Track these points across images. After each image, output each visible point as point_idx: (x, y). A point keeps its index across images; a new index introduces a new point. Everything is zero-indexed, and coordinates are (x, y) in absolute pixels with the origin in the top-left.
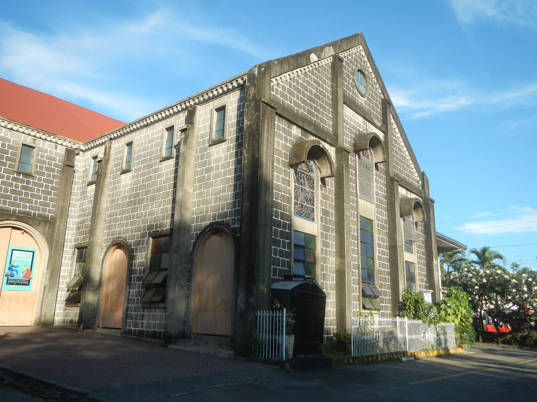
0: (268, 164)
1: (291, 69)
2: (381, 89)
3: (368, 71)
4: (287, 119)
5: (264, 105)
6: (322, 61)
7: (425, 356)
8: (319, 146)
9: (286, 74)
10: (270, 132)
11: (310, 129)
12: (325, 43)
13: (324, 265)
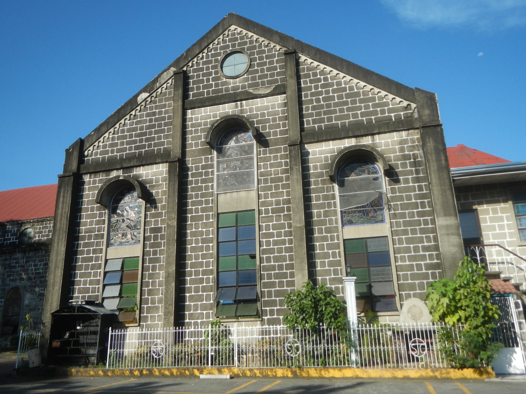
0: (63, 220)
1: (110, 126)
2: (279, 44)
3: (251, 42)
4: (103, 171)
5: (61, 178)
6: (159, 90)
7: (290, 375)
8: (119, 180)
9: (106, 135)
10: (66, 196)
11: (132, 164)
12: (162, 71)
13: (151, 281)
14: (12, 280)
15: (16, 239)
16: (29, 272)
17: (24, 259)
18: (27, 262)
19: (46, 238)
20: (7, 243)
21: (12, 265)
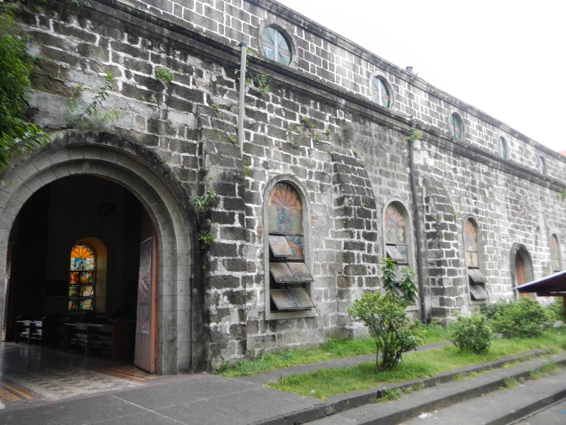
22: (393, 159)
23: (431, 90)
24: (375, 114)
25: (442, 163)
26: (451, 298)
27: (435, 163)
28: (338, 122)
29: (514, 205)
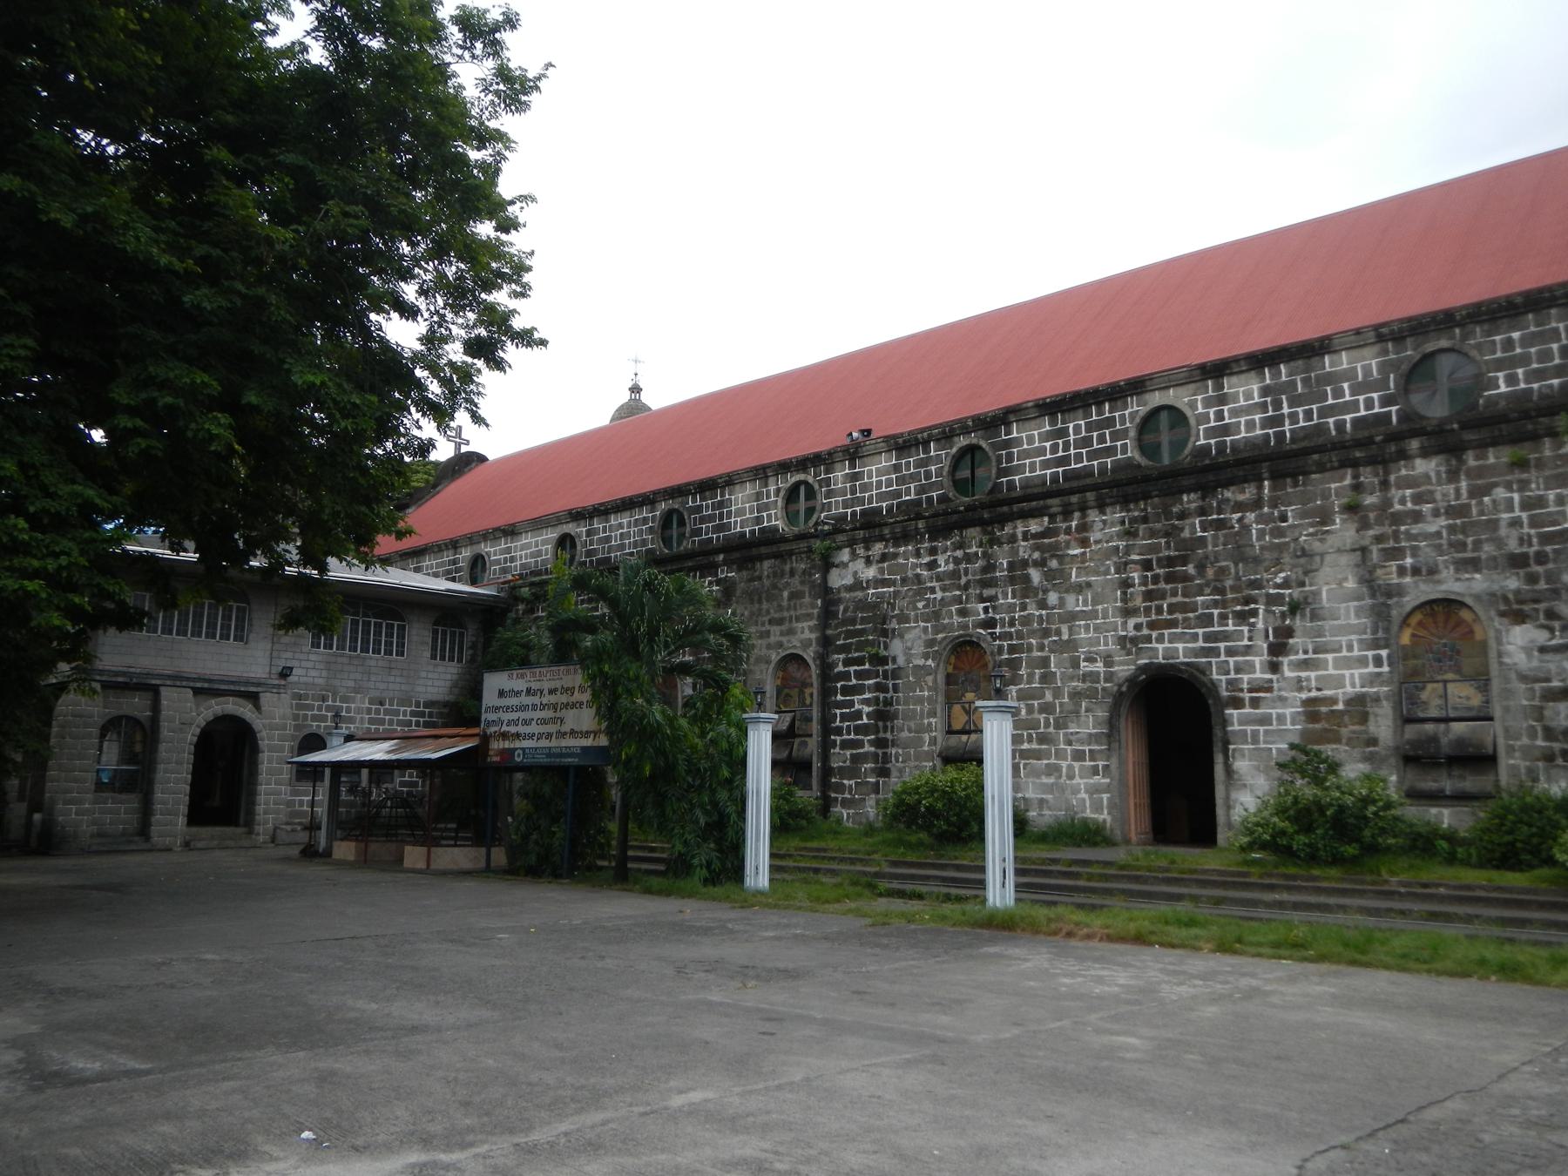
14: (1416, 571)
15: (1386, 401)
16: (1503, 531)
17: (1457, 480)
18: (1476, 492)
19: (1556, 382)
20: (1340, 426)
21: (1398, 507)
22: (794, 596)
23: (896, 443)
24: (763, 550)
25: (898, 564)
26: (845, 782)
27: (881, 571)
28: (718, 582)
29: (1161, 571)
